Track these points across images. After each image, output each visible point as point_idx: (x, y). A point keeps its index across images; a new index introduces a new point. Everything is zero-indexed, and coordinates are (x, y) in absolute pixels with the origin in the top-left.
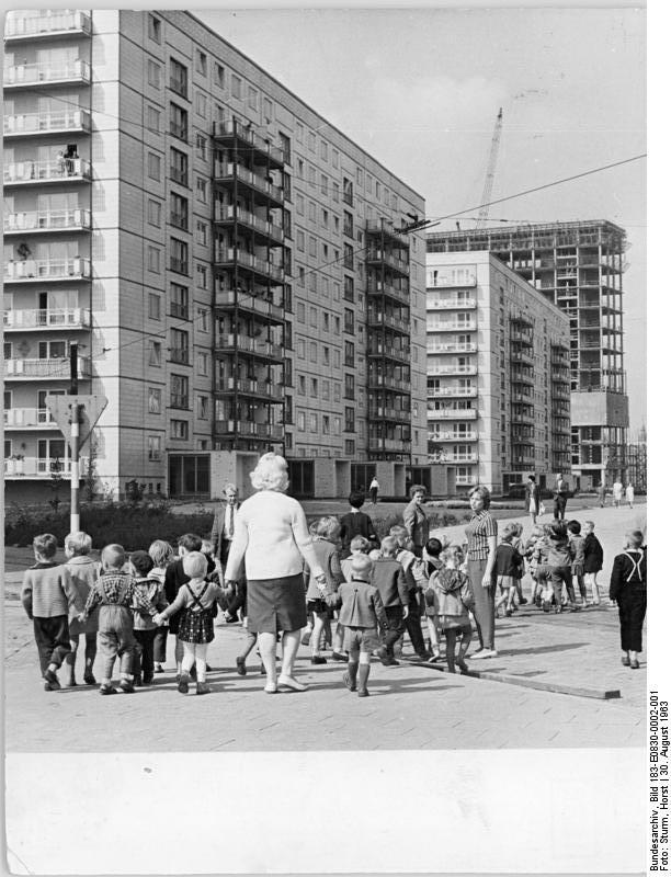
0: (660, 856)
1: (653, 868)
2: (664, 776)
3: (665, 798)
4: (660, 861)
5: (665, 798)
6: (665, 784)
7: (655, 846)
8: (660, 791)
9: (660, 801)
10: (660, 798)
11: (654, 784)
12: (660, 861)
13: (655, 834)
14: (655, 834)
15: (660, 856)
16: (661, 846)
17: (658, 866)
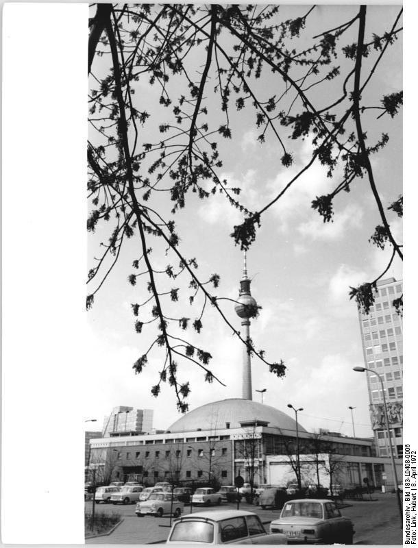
0: (411, 535)
1: (407, 543)
2: (414, 488)
3: (414, 499)
4: (411, 538)
5: (414, 499)
6: (414, 492)
7: (408, 529)
8: (411, 496)
9: (411, 500)
10: (411, 497)
11: (407, 490)
12: (411, 538)
13: (408, 521)
14: (408, 521)
15: (411, 535)
16: (412, 529)
17: (410, 541)
